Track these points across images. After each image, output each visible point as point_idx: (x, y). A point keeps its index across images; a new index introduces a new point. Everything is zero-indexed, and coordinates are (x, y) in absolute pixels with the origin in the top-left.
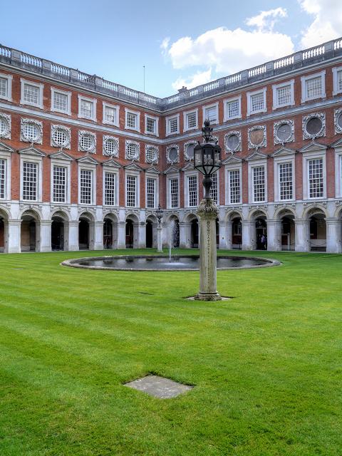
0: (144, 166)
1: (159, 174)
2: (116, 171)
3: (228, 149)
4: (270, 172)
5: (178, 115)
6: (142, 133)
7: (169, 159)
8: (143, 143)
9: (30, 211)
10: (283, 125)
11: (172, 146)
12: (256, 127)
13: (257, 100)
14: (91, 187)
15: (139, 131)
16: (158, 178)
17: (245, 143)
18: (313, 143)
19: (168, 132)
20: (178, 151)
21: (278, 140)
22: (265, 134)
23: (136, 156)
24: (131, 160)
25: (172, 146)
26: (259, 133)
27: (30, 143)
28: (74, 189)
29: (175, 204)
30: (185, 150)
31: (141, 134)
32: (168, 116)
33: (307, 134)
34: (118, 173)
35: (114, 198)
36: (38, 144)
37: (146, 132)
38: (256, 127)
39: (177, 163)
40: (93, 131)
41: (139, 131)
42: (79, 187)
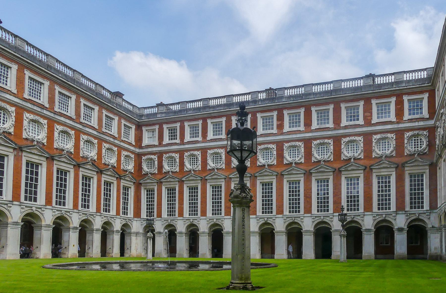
0: (403, 160)
9: (266, 223)
24: (382, 157)
27: (265, 165)
28: (308, 199)
36: (271, 165)
40: (329, 138)
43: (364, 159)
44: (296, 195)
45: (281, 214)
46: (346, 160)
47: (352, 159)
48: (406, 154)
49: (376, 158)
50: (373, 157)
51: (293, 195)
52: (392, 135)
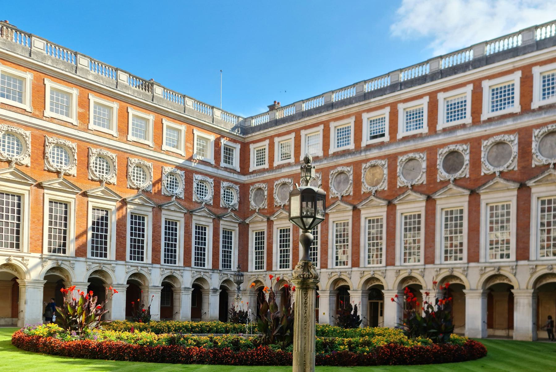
0: (220, 212)
1: (239, 224)
2: (179, 218)
3: (334, 191)
4: (391, 225)
5: (267, 142)
6: (217, 166)
7: (252, 203)
8: (218, 181)
10: (411, 160)
11: (257, 185)
12: (373, 162)
13: (377, 128)
14: (145, 239)
15: (213, 162)
16: (237, 229)
17: (357, 183)
18: (451, 186)
19: (253, 167)
20: (266, 193)
21: (402, 181)
22: (386, 171)
23: (209, 197)
24: (201, 203)
25: (257, 185)
26: (378, 170)
29: (259, 266)
30: (276, 190)
31: (215, 167)
32: (254, 142)
33: (442, 175)
34: (183, 220)
35: (177, 254)
37: (223, 164)
38: (373, 162)
39: (264, 209)
41: (213, 162)
42: (128, 237)
43: (185, 200)
44: (102, 229)
45: (82, 256)
46: (167, 196)
47: (174, 197)
48: (221, 206)
49: (196, 202)
50: (194, 200)
51: (98, 229)
52: (212, 180)
